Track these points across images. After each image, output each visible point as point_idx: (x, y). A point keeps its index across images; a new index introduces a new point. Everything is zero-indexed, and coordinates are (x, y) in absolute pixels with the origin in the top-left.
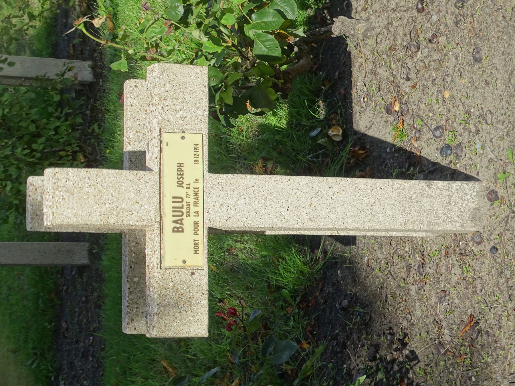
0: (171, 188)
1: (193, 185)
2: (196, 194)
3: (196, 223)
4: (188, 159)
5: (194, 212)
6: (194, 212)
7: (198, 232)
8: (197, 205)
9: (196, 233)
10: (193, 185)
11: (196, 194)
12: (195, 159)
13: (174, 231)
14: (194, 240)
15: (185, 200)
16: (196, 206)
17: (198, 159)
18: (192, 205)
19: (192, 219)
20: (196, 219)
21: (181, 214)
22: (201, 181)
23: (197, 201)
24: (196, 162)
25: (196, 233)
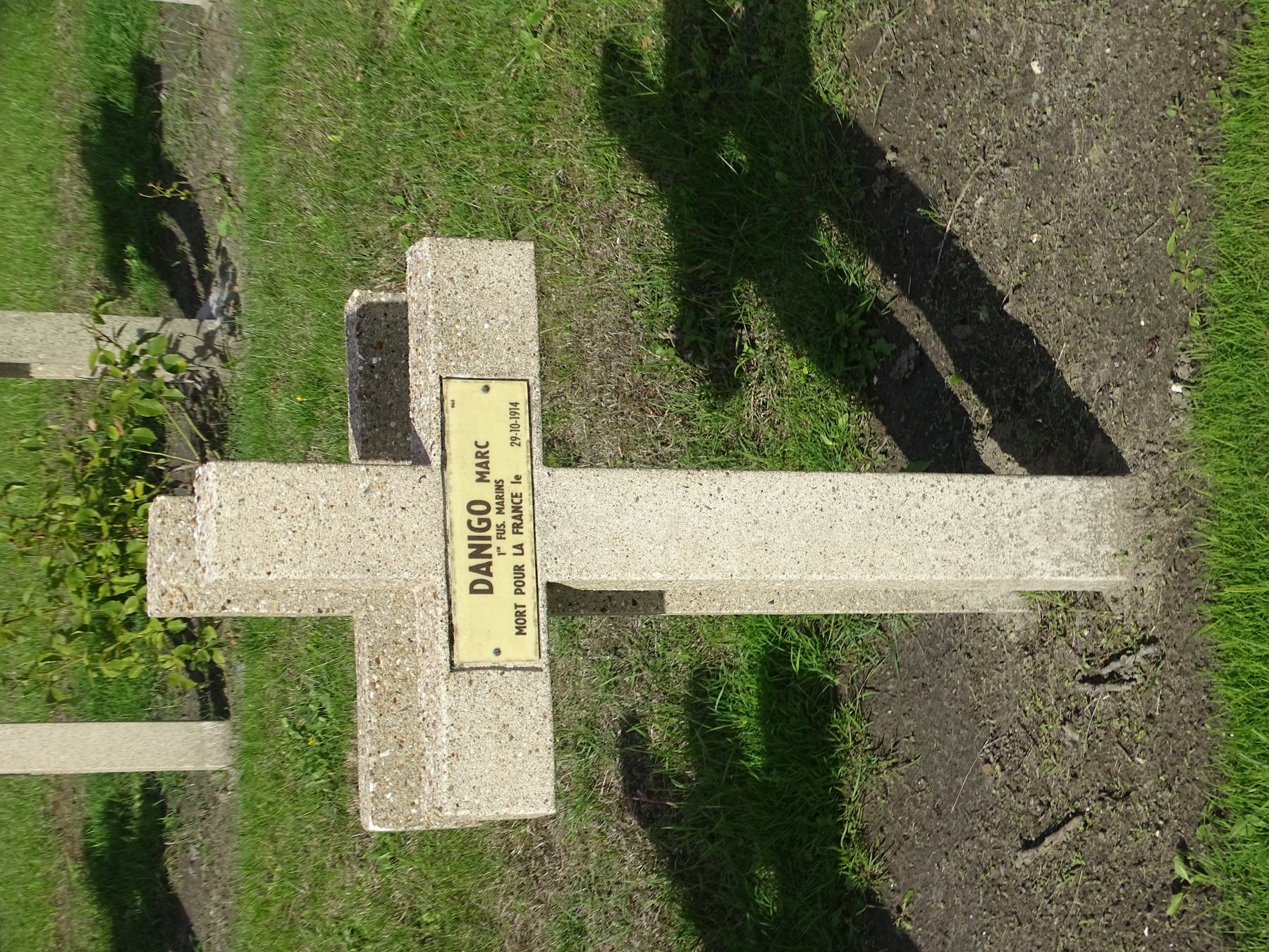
1: (509, 489)
2: (517, 509)
3: (519, 569)
4: (497, 434)
9: (519, 591)
11: (517, 509)
13: (472, 591)
14: (516, 606)
16: (518, 533)
18: (509, 529)
20: (519, 561)
22: (525, 480)
25: (519, 591)
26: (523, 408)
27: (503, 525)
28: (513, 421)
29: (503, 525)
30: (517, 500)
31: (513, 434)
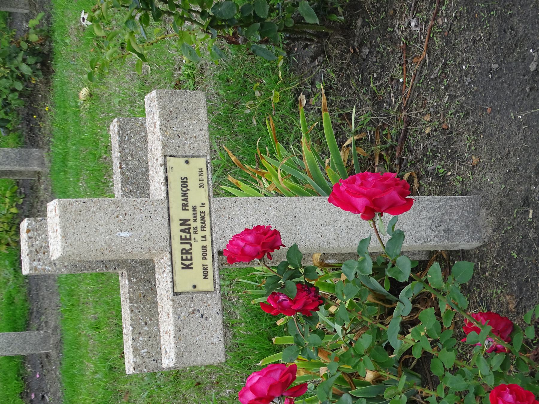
0: (177, 214)
1: (199, 209)
2: (203, 218)
5: (202, 237)
6: (202, 237)
8: (205, 229)
9: (204, 258)
11: (203, 218)
14: (203, 265)
15: (193, 225)
16: (203, 230)
17: (203, 182)
18: (199, 229)
20: (204, 243)
22: (207, 205)
23: (204, 225)
24: (201, 186)
25: (204, 258)
26: (205, 170)
27: (196, 227)
28: (200, 177)
29: (196, 227)
30: (203, 215)
31: (201, 182)
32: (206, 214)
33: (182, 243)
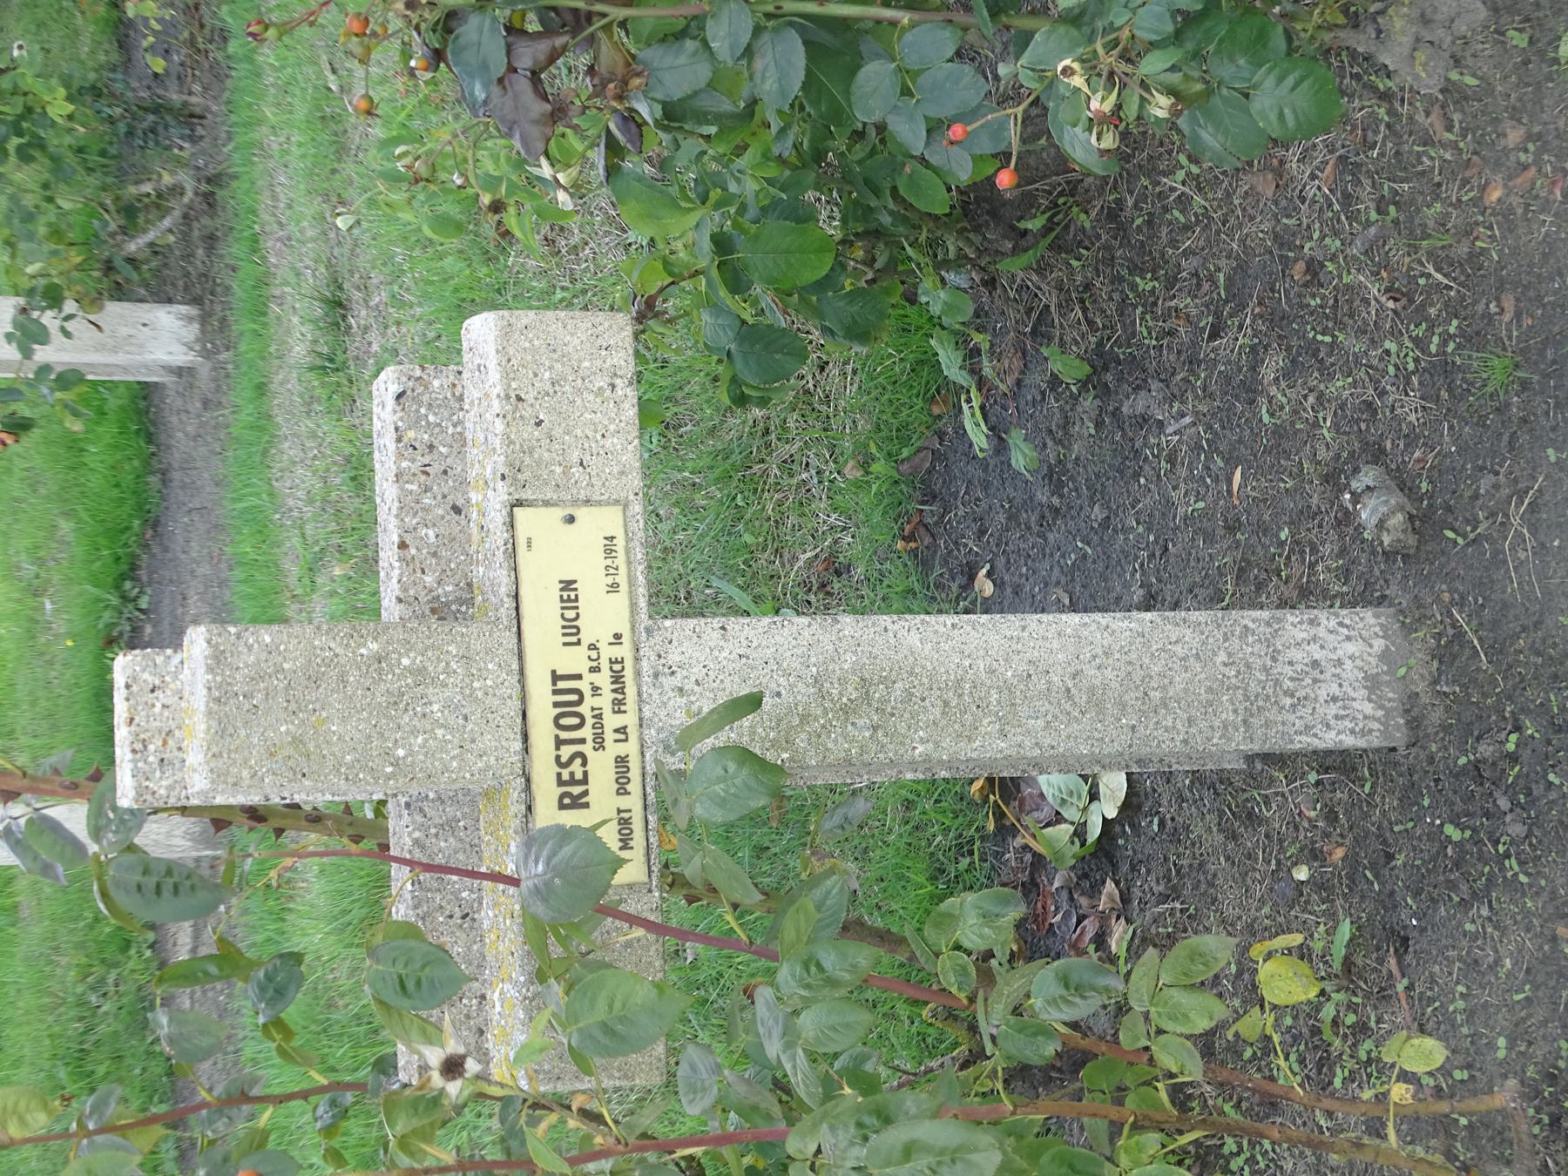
1: (607, 652)
2: (617, 678)
5: (616, 731)
6: (616, 731)
7: (629, 787)
9: (622, 791)
10: (607, 652)
11: (617, 678)
12: (610, 580)
14: (619, 811)
16: (620, 712)
19: (613, 749)
20: (621, 749)
21: (574, 697)
23: (620, 697)
24: (614, 588)
26: (620, 543)
28: (609, 562)
30: (617, 667)
32: (629, 664)
33: (556, 705)
